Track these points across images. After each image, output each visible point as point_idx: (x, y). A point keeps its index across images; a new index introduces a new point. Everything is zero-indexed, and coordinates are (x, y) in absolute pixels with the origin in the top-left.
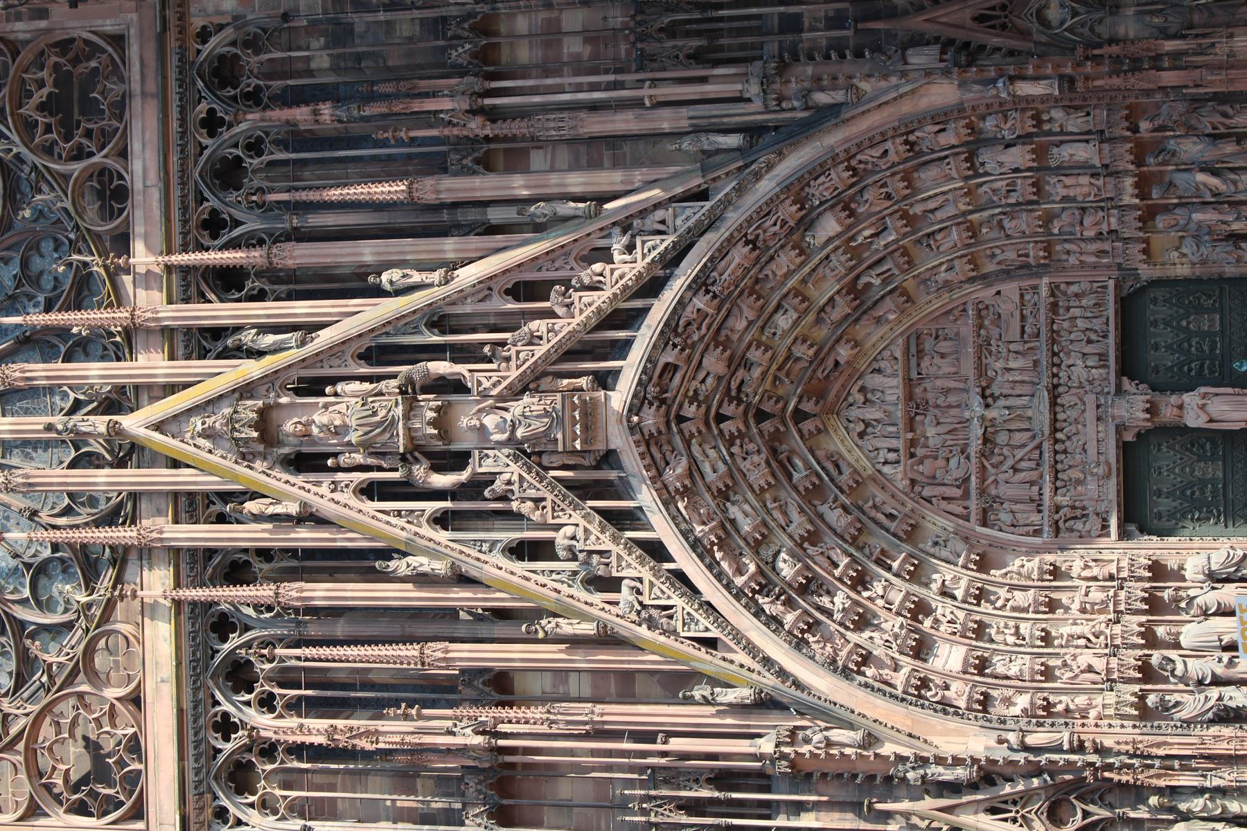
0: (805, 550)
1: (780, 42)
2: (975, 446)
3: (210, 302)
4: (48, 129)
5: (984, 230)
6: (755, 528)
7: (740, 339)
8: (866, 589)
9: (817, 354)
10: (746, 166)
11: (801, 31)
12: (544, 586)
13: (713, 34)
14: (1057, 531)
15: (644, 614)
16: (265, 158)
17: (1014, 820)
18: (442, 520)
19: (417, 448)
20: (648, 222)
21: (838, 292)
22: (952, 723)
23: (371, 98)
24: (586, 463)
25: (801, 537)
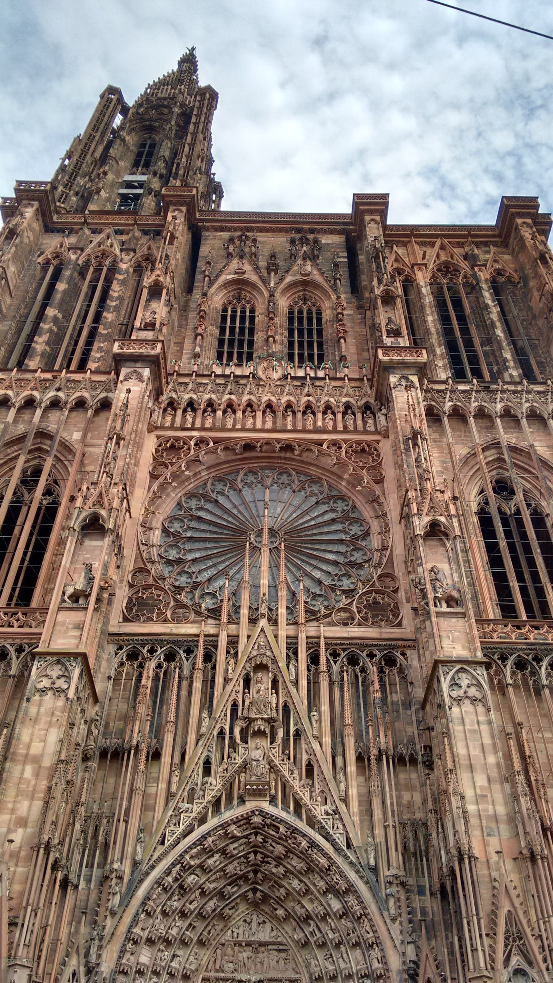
1: (413, 885)
4: (367, 601)
7: (288, 863)
8: (179, 918)
9: (281, 899)
10: (361, 866)
12: (193, 771)
15: (177, 813)
16: (359, 674)
18: (222, 733)
19: (250, 723)
20: (338, 822)
21: (307, 910)
24: (241, 791)
25: (204, 888)
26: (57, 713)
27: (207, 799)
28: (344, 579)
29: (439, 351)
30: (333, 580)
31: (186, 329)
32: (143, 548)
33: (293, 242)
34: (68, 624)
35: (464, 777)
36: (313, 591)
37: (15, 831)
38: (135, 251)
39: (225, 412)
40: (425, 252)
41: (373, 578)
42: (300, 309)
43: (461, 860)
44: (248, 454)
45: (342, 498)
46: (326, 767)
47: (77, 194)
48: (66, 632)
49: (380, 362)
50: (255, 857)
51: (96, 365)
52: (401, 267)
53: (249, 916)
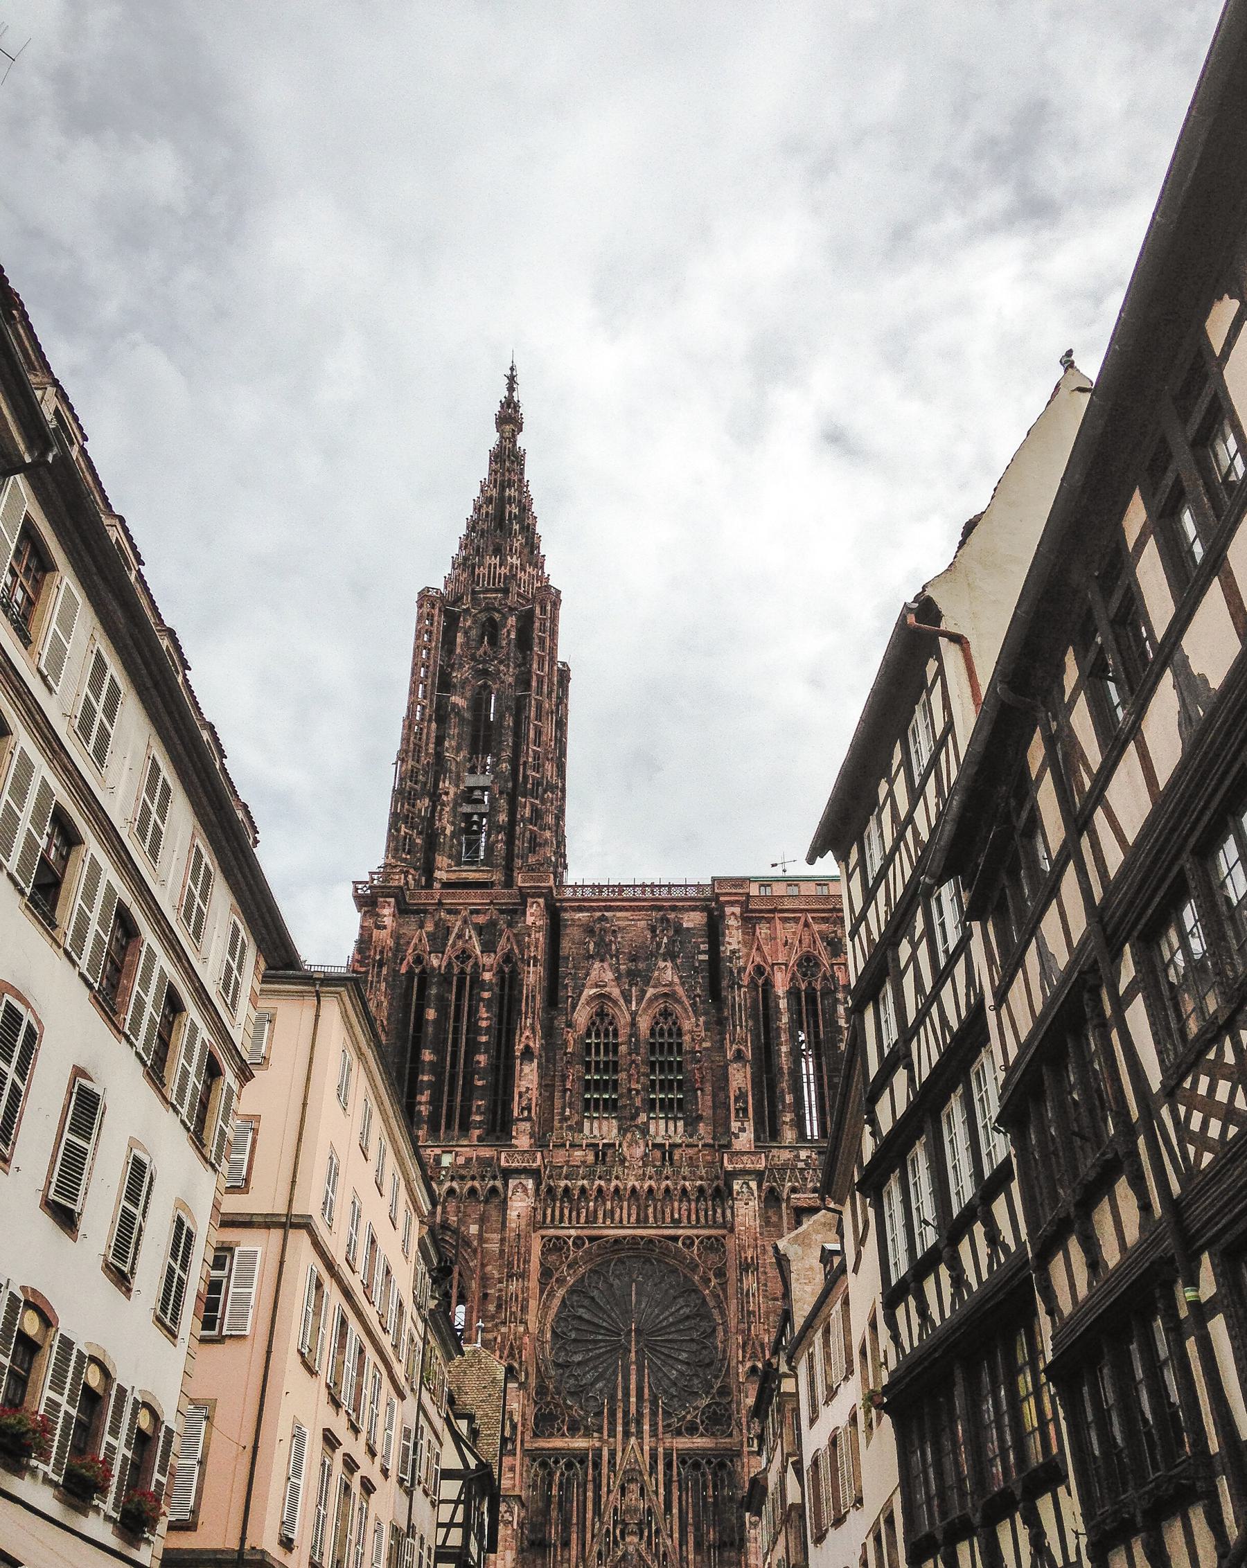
18: (608, 1530)
29: (789, 1099)
31: (554, 1065)
32: (540, 1361)
33: (653, 929)
38: (495, 952)
39: (596, 1200)
40: (787, 941)
41: (713, 1387)
42: (662, 1029)
44: (616, 1247)
45: (696, 1291)
47: (419, 833)
49: (726, 1171)
51: (477, 1132)
52: (762, 963)
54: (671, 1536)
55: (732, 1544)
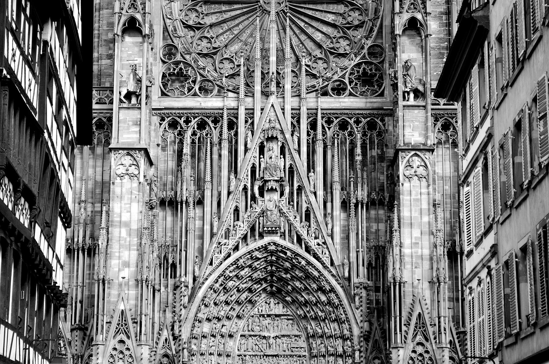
0: (235, 288)
2: (263, 334)
3: (307, 120)
4: (358, 72)
5: (321, 339)
6: (242, 276)
10: (339, 277)
11: (376, 292)
13: (376, 268)
14: (239, 356)
17: (163, 346)
18: (245, 189)
21: (305, 299)
22: (189, 330)
23: (362, 170)
24: (260, 230)
25: (239, 288)
26: (134, 192)
27: (238, 237)
28: (341, 40)
30: (332, 42)
32: (168, 21)
34: (129, 121)
35: (405, 231)
36: (314, 54)
37: (124, 270)
43: (395, 283)
46: (319, 213)
48: (128, 129)
50: (272, 268)
53: (269, 300)
54: (315, 194)
55: (381, 203)
